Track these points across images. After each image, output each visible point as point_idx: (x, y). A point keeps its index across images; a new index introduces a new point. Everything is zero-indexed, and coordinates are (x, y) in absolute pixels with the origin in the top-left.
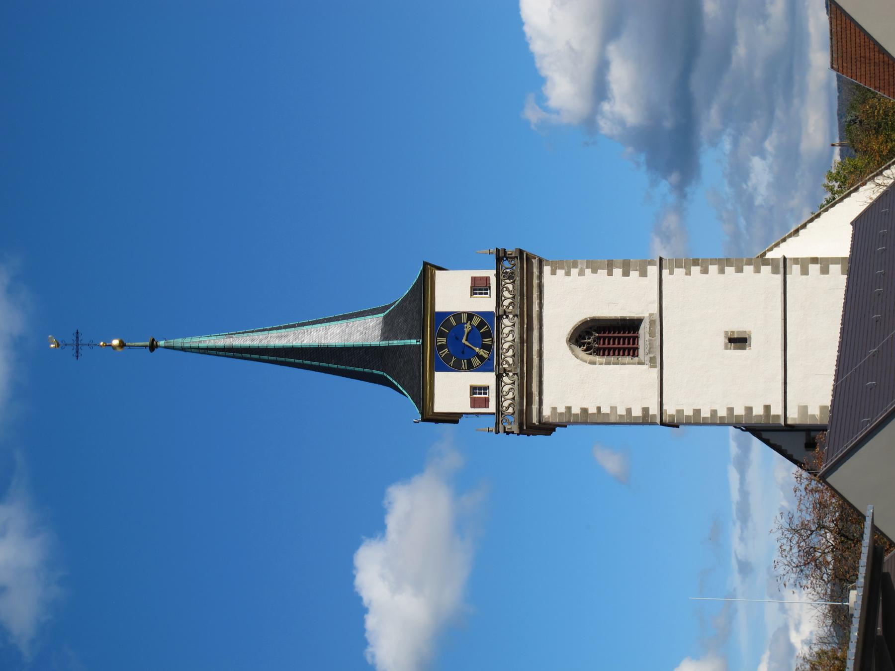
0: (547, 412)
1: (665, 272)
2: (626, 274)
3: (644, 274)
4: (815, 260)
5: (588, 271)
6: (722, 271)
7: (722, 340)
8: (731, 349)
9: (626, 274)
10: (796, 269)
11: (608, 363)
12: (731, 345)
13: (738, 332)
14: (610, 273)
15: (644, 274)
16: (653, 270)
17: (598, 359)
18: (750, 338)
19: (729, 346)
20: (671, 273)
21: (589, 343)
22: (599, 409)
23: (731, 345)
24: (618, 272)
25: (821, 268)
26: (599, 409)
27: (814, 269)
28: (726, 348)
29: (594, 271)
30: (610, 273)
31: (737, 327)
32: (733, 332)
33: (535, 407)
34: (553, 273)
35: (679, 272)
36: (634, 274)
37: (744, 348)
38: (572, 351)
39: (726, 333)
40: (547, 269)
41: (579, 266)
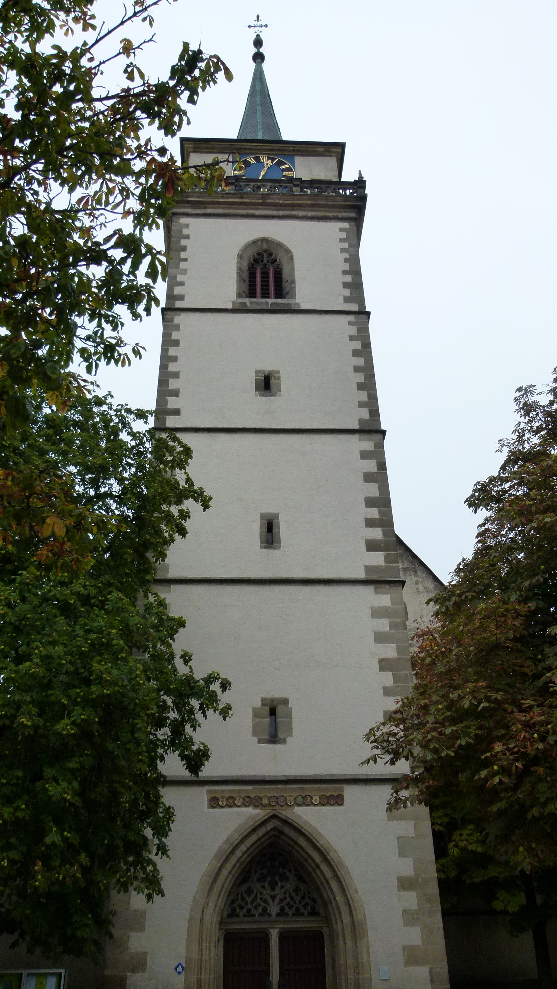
0: (184, 220)
1: (351, 318)
2: (346, 285)
3: (347, 300)
4: (382, 466)
5: (347, 256)
6: (357, 369)
7: (267, 367)
8: (256, 376)
9: (346, 285)
10: (368, 445)
11: (240, 269)
12: (262, 376)
13: (279, 384)
14: (345, 273)
15: (347, 300)
16: (354, 307)
17: (245, 265)
18: (272, 395)
19: (260, 375)
20: (350, 323)
21: (262, 261)
22: (186, 260)
23: (262, 376)
24: (348, 279)
25: (373, 474)
26: (186, 260)
27: (371, 466)
28: (258, 372)
29: (346, 260)
30: (345, 273)
31: (286, 383)
32: (279, 378)
33: (189, 211)
34: (341, 230)
35: (353, 331)
36: (347, 292)
37: (257, 388)
38: (255, 242)
39: (278, 372)
40: (346, 225)
41: (351, 249)
